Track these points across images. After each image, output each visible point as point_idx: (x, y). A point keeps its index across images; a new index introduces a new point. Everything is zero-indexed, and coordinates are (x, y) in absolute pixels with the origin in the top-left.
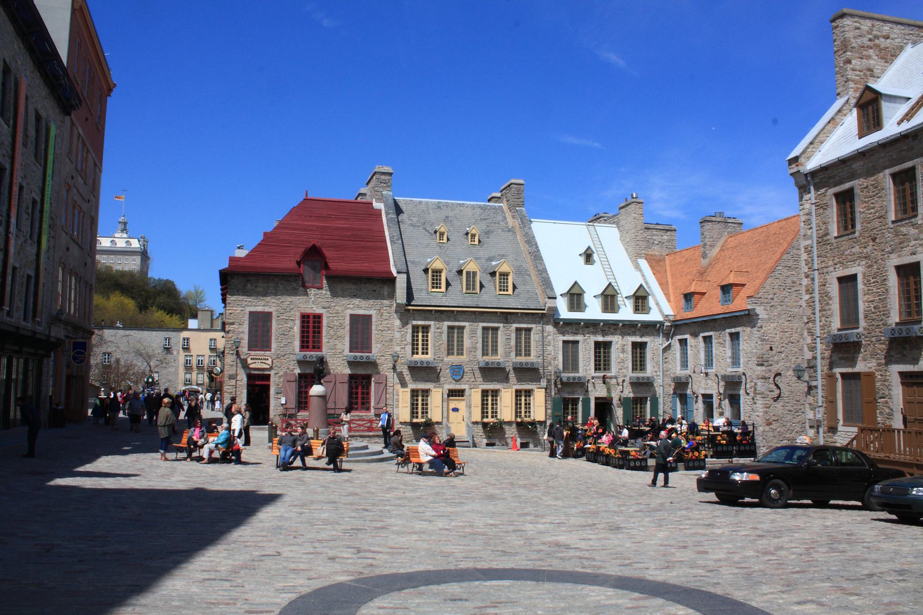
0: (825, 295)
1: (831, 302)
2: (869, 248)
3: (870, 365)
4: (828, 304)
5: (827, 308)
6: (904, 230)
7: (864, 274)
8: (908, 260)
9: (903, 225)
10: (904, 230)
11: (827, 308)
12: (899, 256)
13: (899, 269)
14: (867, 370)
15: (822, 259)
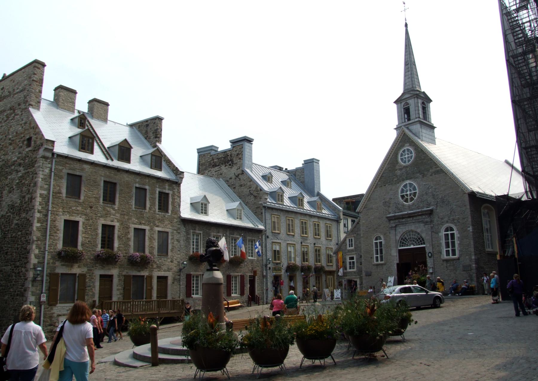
0: (54, 227)
1: (58, 232)
2: (88, 211)
3: (83, 270)
4: (56, 232)
5: (55, 235)
6: (108, 209)
7: (83, 223)
8: (109, 223)
9: (108, 207)
10: (108, 209)
11: (55, 235)
12: (105, 220)
13: (104, 226)
14: (80, 272)
15: (54, 206)
